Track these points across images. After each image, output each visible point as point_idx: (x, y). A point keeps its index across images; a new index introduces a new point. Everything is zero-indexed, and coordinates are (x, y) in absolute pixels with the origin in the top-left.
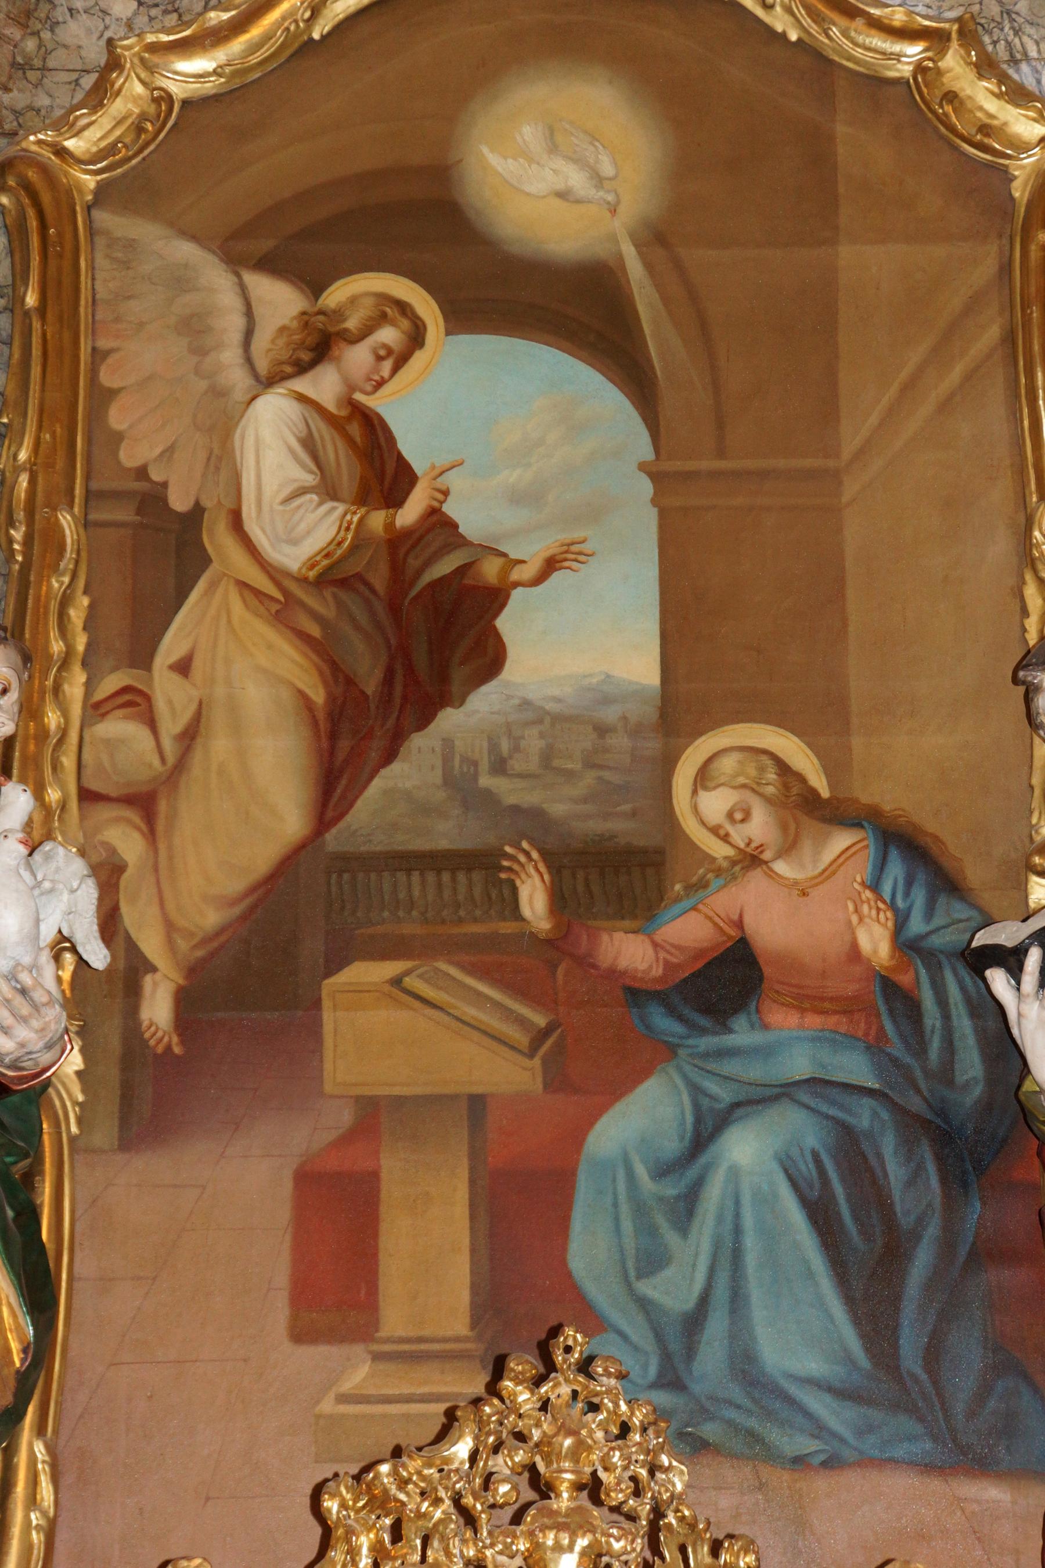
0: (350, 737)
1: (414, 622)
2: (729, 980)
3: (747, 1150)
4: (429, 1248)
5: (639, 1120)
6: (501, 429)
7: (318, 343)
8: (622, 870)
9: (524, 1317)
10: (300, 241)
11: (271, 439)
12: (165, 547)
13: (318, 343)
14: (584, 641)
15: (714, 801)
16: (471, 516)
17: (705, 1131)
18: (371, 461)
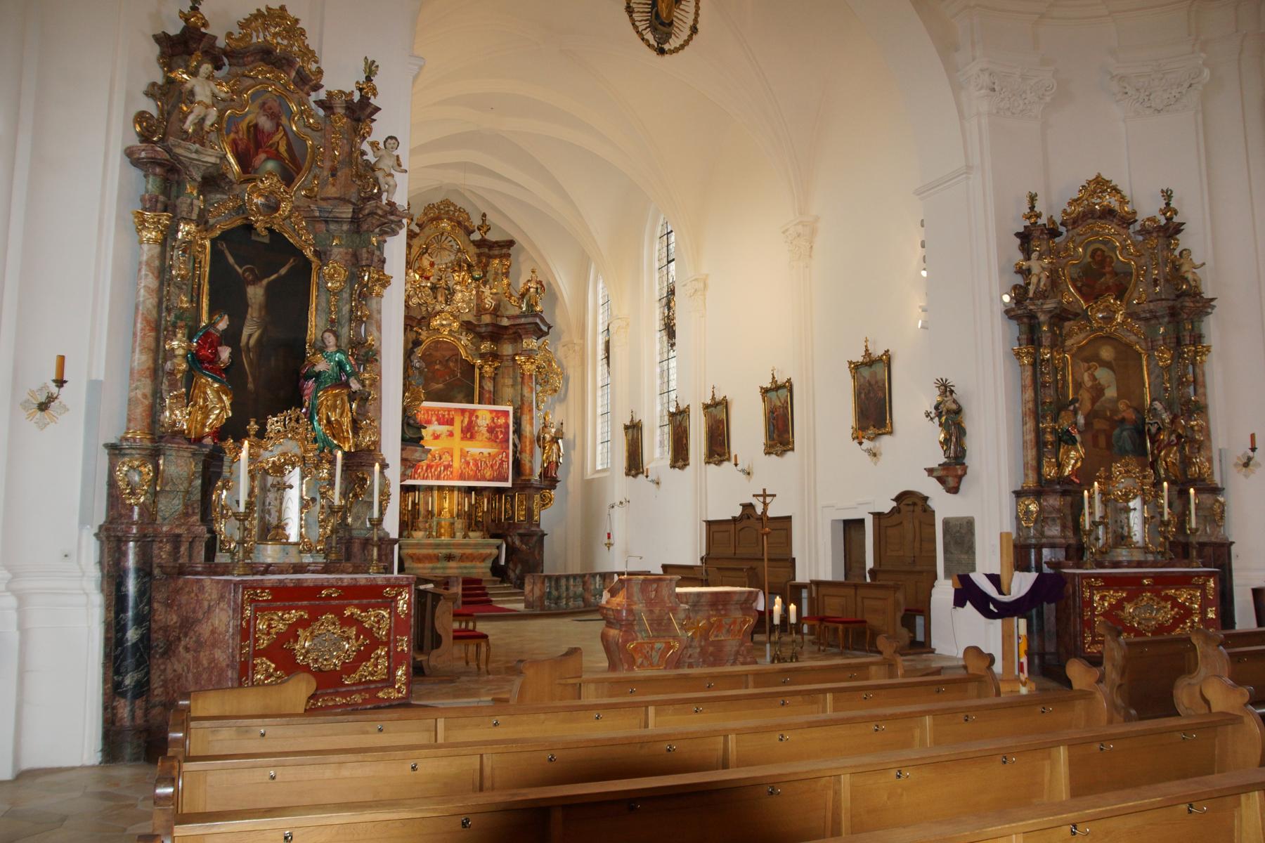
0: (1094, 401)
1: (1098, 391)
2: (1123, 420)
3: (1125, 433)
4: (1102, 441)
5: (1117, 432)
6: (1103, 375)
7: (1089, 368)
8: (1115, 411)
9: (1109, 445)
10: (1086, 360)
11: (1086, 377)
12: (1078, 385)
13: (1089, 368)
14: (1111, 393)
15: (1121, 406)
16: (1102, 382)
17: (1122, 431)
18: (1094, 378)
